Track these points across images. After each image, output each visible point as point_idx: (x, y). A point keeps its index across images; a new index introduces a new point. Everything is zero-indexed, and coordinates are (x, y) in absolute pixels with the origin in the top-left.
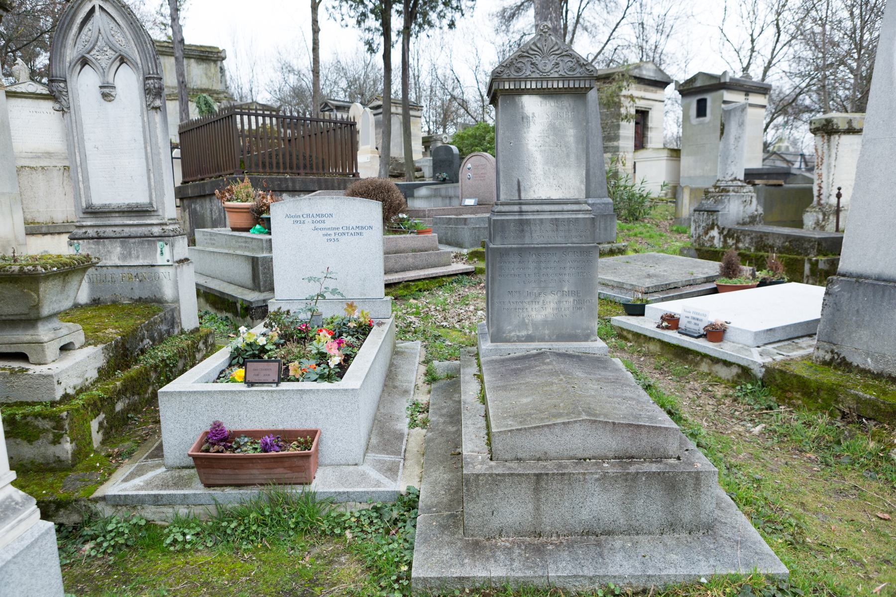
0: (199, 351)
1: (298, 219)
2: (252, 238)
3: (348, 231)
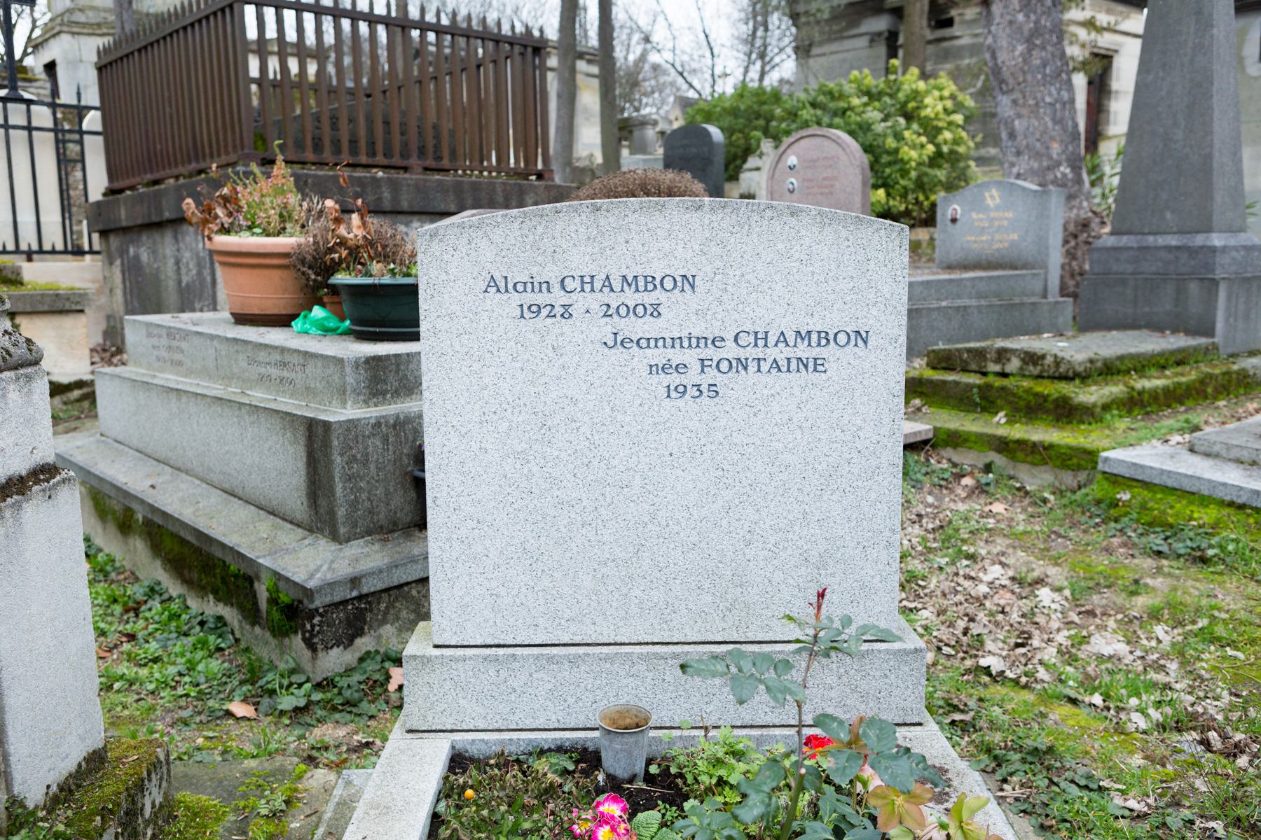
2: (306, 354)
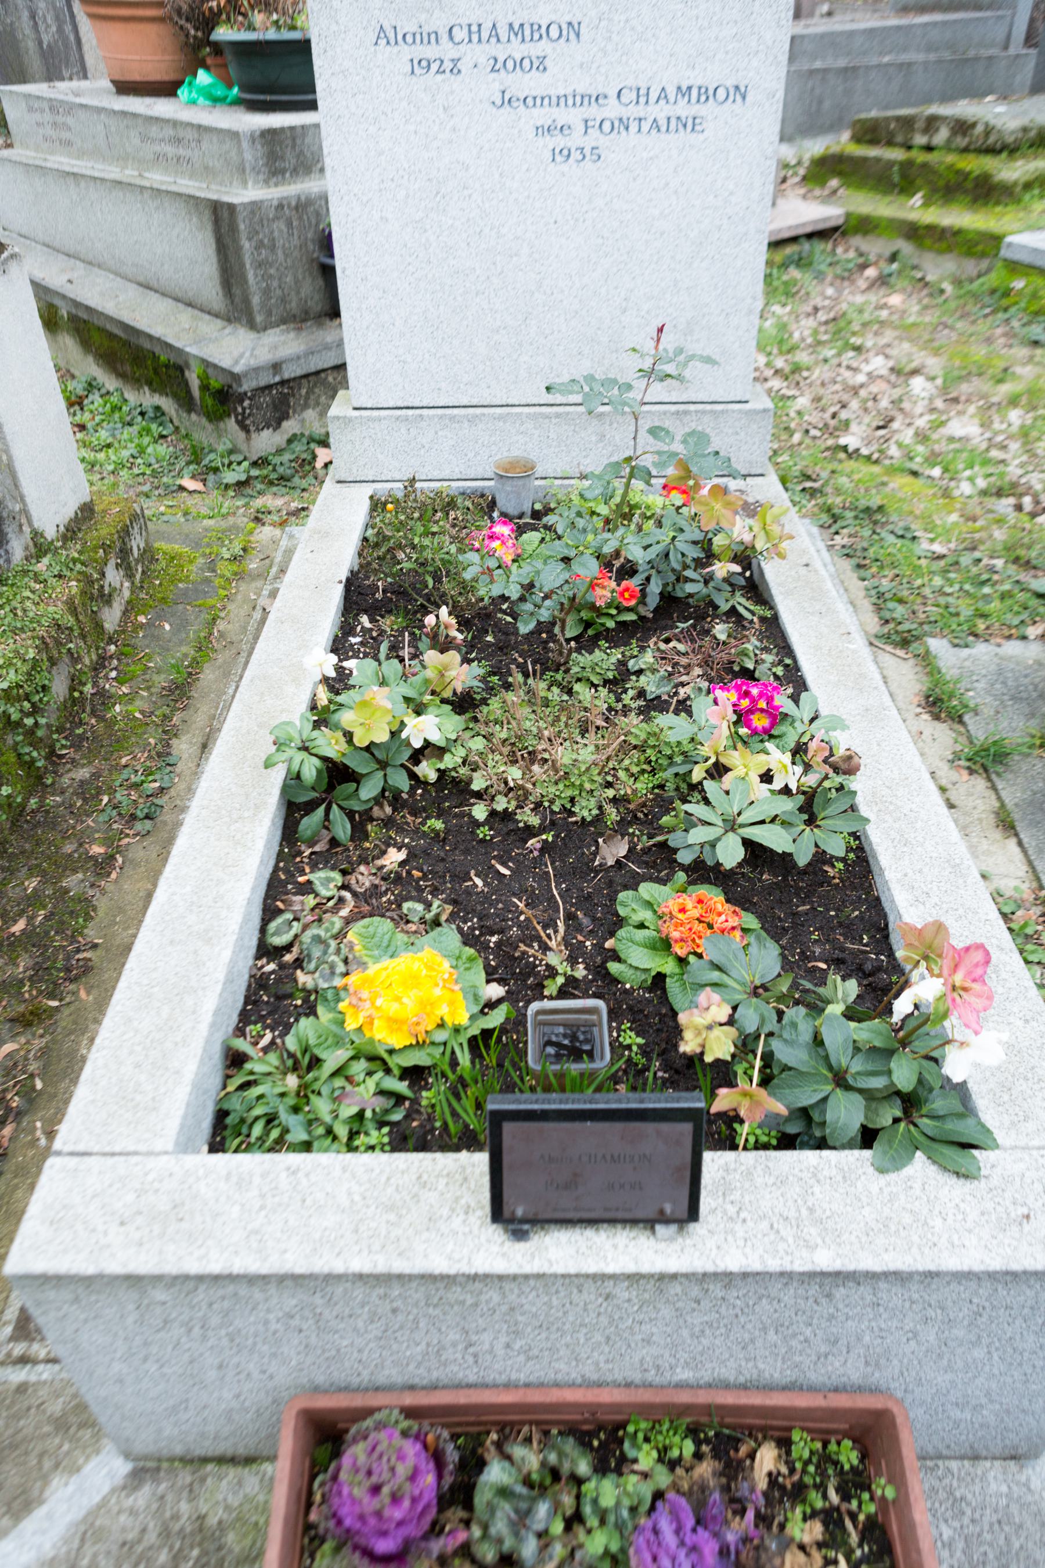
0: (107, 599)
1: (430, 52)
2: (200, 128)
3: (640, 111)
